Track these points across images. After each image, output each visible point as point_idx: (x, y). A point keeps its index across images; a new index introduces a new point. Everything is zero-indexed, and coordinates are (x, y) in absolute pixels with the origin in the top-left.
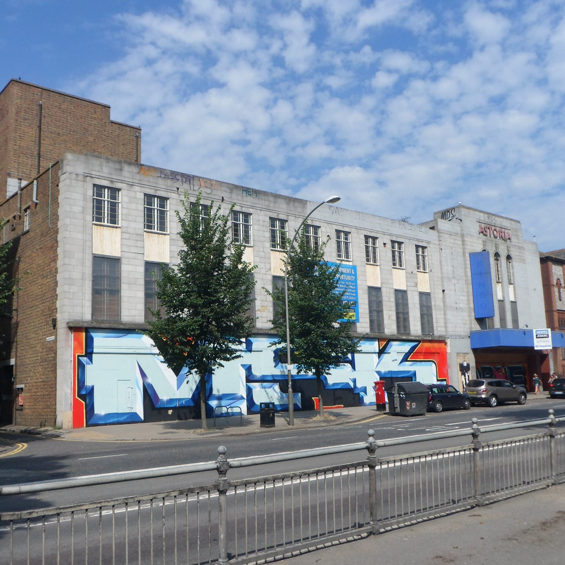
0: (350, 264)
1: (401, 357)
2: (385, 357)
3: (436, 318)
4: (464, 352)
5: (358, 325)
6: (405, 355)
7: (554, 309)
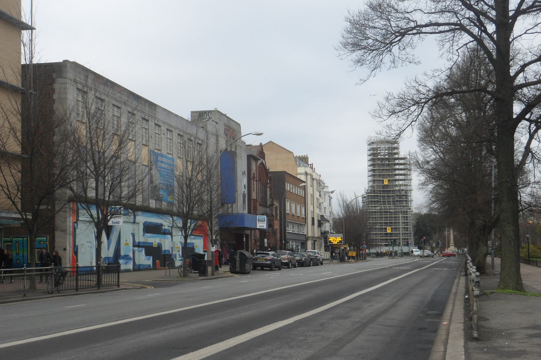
0: (171, 156)
7: (252, 198)
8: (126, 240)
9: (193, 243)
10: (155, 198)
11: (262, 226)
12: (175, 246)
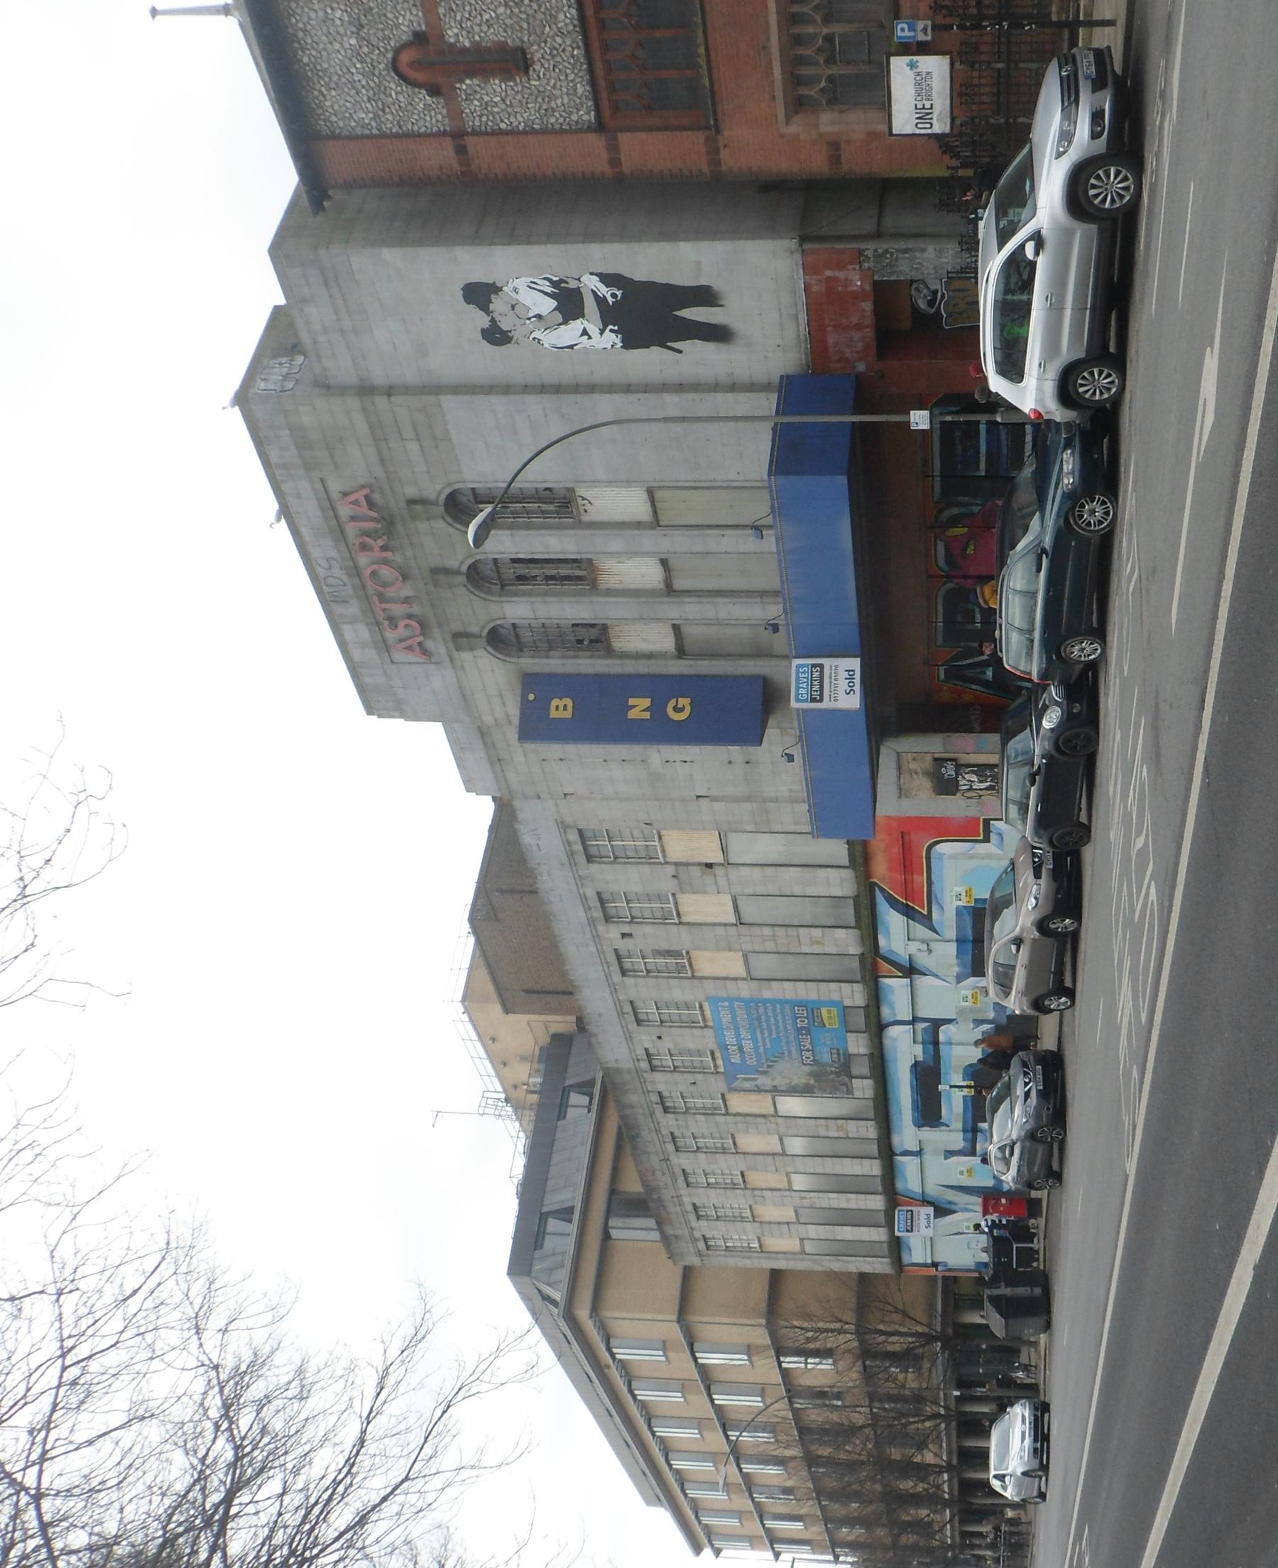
1: (920, 931)
2: (923, 960)
3: (796, 824)
4: (894, 772)
5: (848, 1003)
6: (913, 920)
8: (962, 1173)
9: (959, 911)
10: (846, 1079)
11: (850, 679)
12: (971, 1010)
